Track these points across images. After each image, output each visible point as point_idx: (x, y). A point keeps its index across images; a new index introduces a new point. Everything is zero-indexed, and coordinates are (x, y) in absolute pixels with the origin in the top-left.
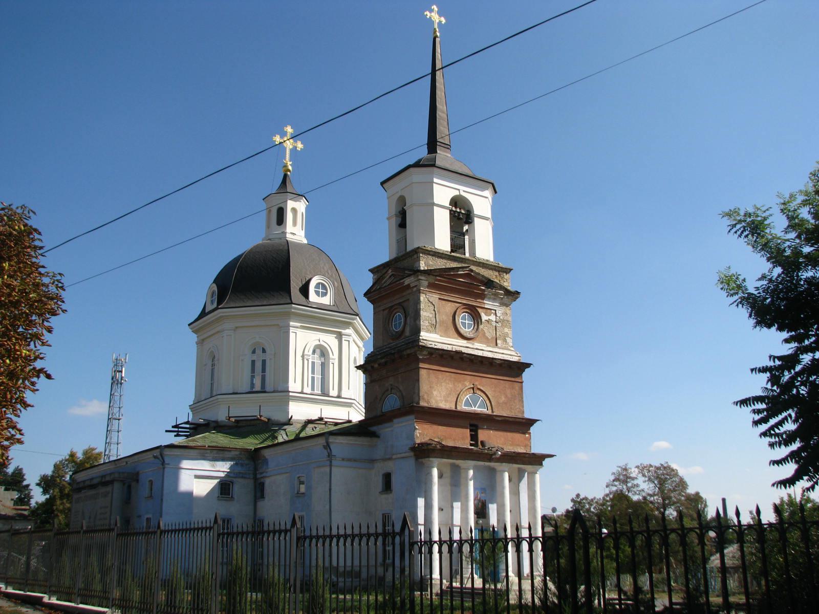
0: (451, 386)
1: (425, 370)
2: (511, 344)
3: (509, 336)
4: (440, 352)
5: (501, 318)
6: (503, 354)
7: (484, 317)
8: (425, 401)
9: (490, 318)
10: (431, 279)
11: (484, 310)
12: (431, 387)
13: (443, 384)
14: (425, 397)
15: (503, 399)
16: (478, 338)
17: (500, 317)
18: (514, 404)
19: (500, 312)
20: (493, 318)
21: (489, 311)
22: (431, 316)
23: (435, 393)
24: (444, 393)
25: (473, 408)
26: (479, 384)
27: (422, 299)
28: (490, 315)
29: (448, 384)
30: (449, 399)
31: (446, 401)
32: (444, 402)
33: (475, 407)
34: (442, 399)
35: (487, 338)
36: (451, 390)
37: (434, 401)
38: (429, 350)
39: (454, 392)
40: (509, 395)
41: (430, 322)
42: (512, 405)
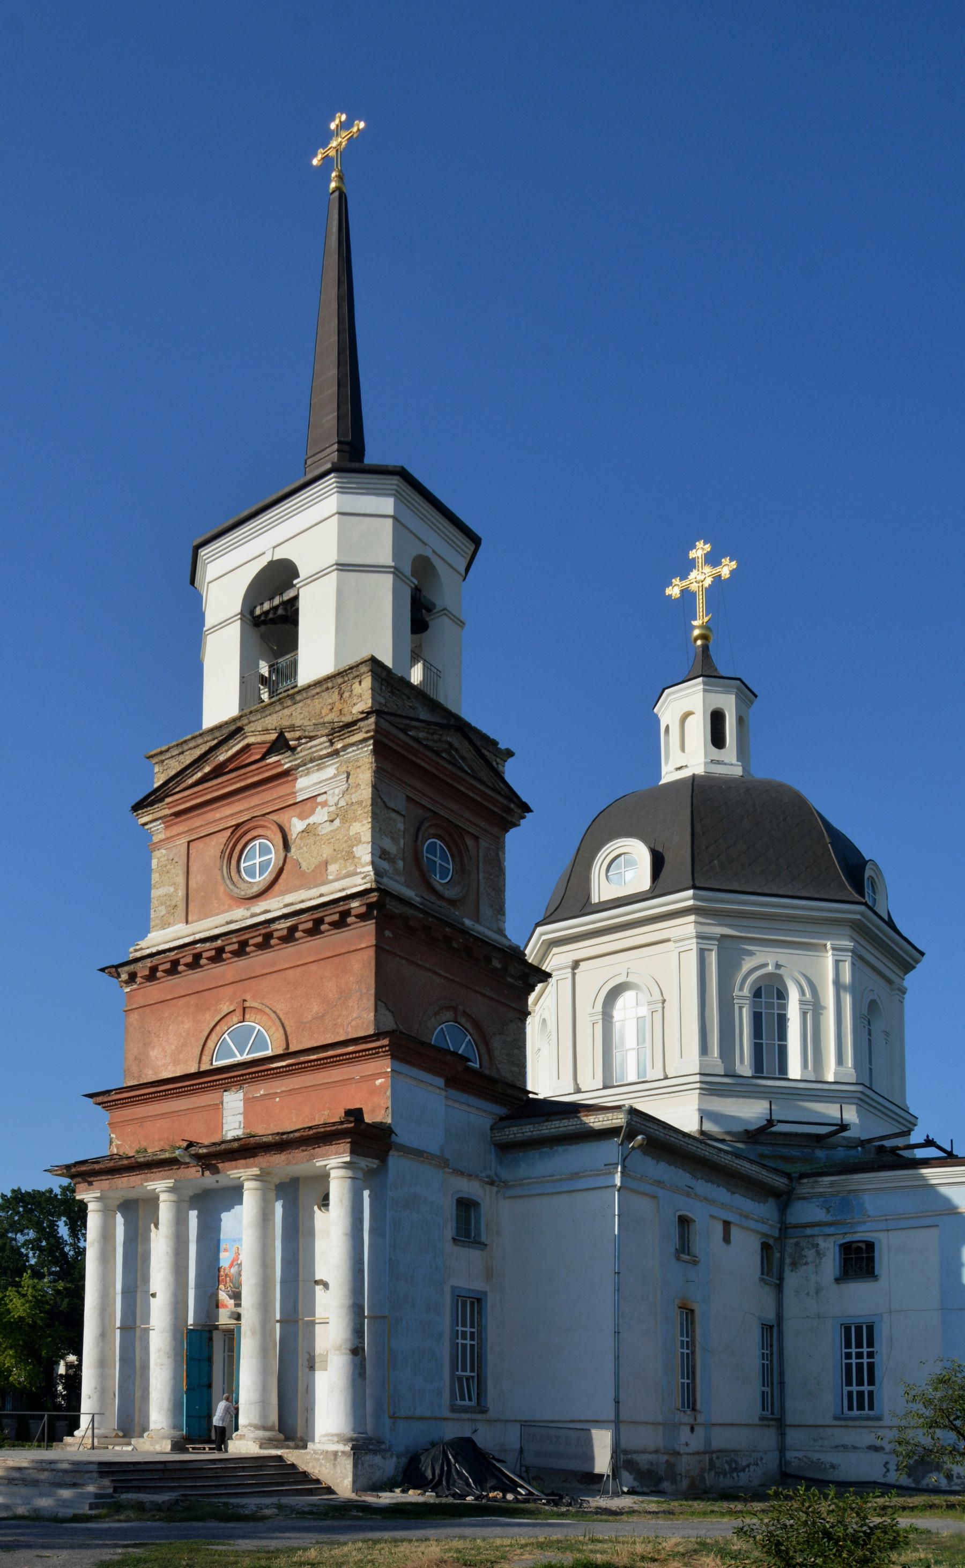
0: (188, 1025)
1: (136, 1012)
2: (368, 858)
3: (363, 839)
4: (148, 963)
5: (342, 803)
6: (321, 895)
7: (296, 826)
8: (134, 1078)
9: (311, 820)
10: (162, 810)
11: (298, 809)
12: (145, 1044)
13: (171, 1028)
14: (134, 1069)
15: (316, 1008)
16: (277, 887)
17: (336, 804)
18: (344, 1013)
19: (337, 791)
20: (320, 816)
21: (309, 804)
22: (172, 889)
23: (154, 1053)
24: (173, 1047)
25: (239, 1058)
26: (254, 998)
27: (154, 862)
28: (312, 812)
29: (183, 1023)
30: (181, 1056)
31: (176, 1062)
32: (170, 1068)
33: (241, 1055)
34: (168, 1060)
35: (303, 873)
36: (188, 1034)
37: (150, 1072)
38: (126, 968)
39: (193, 1036)
40: (332, 995)
41: (168, 903)
42: (339, 1016)
